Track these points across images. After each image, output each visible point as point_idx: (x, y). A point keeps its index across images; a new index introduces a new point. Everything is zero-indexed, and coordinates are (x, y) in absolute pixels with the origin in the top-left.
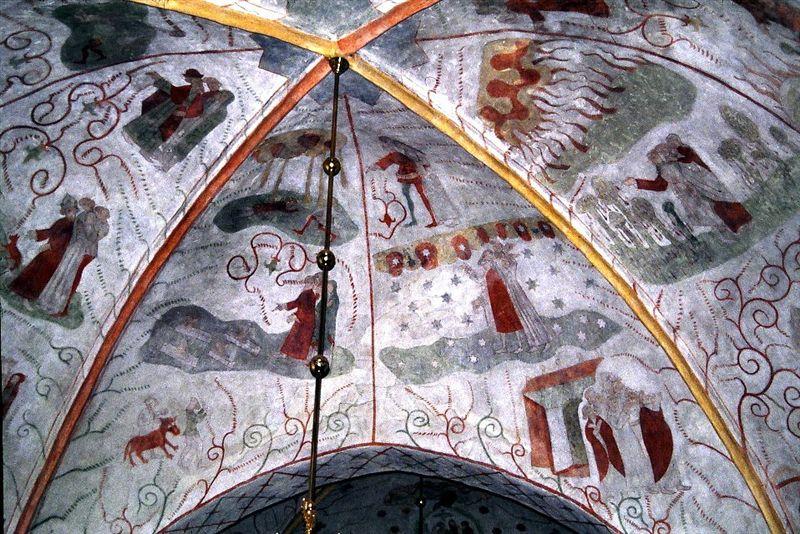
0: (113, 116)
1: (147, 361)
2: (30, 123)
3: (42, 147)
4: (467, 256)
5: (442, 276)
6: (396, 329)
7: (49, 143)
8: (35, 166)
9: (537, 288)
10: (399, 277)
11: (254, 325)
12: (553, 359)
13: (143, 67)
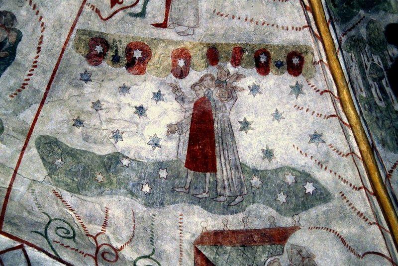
4: (182, 74)
5: (144, 87)
6: (68, 121)
9: (250, 131)
10: (95, 68)
12: (241, 216)
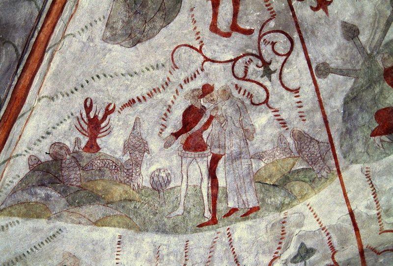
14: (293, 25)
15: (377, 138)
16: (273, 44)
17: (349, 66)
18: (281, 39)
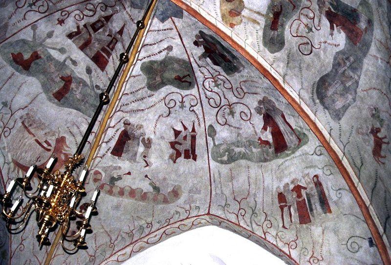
0: (222, 77)
1: (340, 119)
2: (217, 109)
3: (230, 109)
7: (230, 106)
8: (237, 115)
11: (337, 53)
13: (195, 61)
14: (52, 12)
15: (11, 56)
16: (43, 5)
17: (37, 37)
18: (46, 8)
